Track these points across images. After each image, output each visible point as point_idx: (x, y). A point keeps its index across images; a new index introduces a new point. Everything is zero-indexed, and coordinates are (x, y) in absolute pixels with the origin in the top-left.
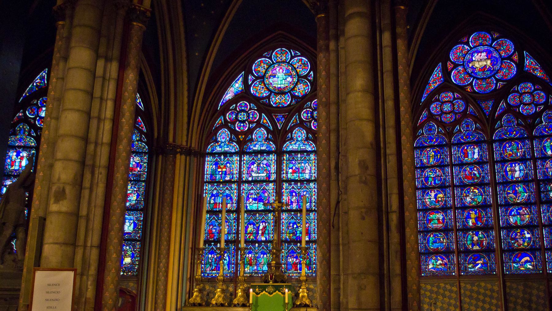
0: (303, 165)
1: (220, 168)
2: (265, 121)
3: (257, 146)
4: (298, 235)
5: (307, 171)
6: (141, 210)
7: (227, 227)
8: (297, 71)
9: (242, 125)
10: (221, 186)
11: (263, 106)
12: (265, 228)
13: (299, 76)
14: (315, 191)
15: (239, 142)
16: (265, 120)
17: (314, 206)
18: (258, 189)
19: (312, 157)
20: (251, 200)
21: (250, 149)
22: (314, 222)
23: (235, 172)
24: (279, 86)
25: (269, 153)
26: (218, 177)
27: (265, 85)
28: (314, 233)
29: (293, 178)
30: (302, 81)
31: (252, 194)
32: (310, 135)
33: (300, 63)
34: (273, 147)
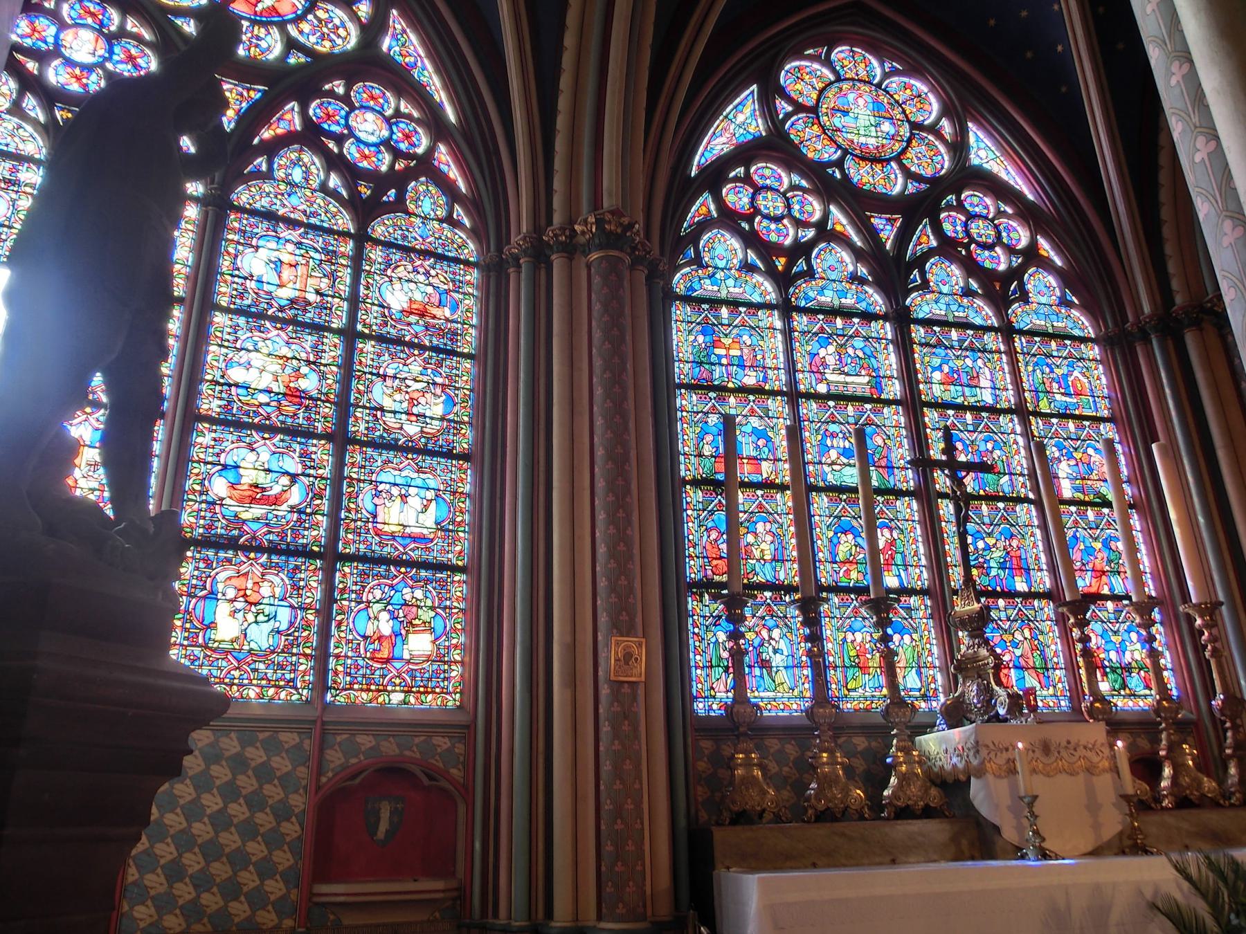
0: (969, 362)
1: (724, 346)
2: (838, 228)
3: (828, 293)
4: (993, 573)
5: (984, 382)
6: (465, 457)
7: (769, 538)
8: (904, 111)
9: (773, 226)
10: (732, 400)
11: (828, 183)
12: (892, 543)
13: (916, 126)
14: (1016, 442)
15: (771, 273)
16: (839, 219)
17: (1024, 485)
18: (851, 420)
19: (992, 341)
20: (833, 454)
21: (806, 298)
22: (1033, 535)
23: (769, 363)
24: (863, 140)
25: (868, 317)
26: (718, 372)
27: (823, 127)
28: (1040, 570)
29: (947, 397)
30: (923, 139)
31: (833, 435)
32: (974, 285)
33: (908, 91)
34: (876, 300)
